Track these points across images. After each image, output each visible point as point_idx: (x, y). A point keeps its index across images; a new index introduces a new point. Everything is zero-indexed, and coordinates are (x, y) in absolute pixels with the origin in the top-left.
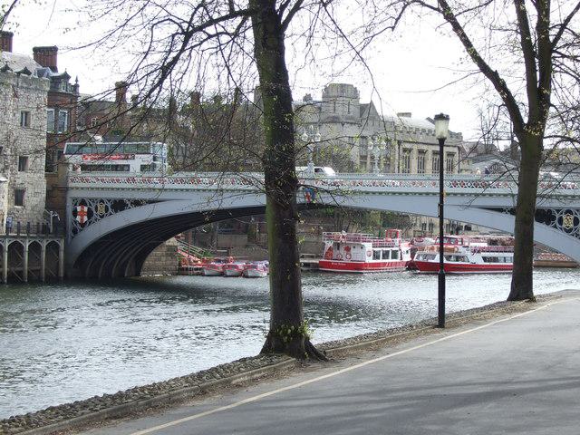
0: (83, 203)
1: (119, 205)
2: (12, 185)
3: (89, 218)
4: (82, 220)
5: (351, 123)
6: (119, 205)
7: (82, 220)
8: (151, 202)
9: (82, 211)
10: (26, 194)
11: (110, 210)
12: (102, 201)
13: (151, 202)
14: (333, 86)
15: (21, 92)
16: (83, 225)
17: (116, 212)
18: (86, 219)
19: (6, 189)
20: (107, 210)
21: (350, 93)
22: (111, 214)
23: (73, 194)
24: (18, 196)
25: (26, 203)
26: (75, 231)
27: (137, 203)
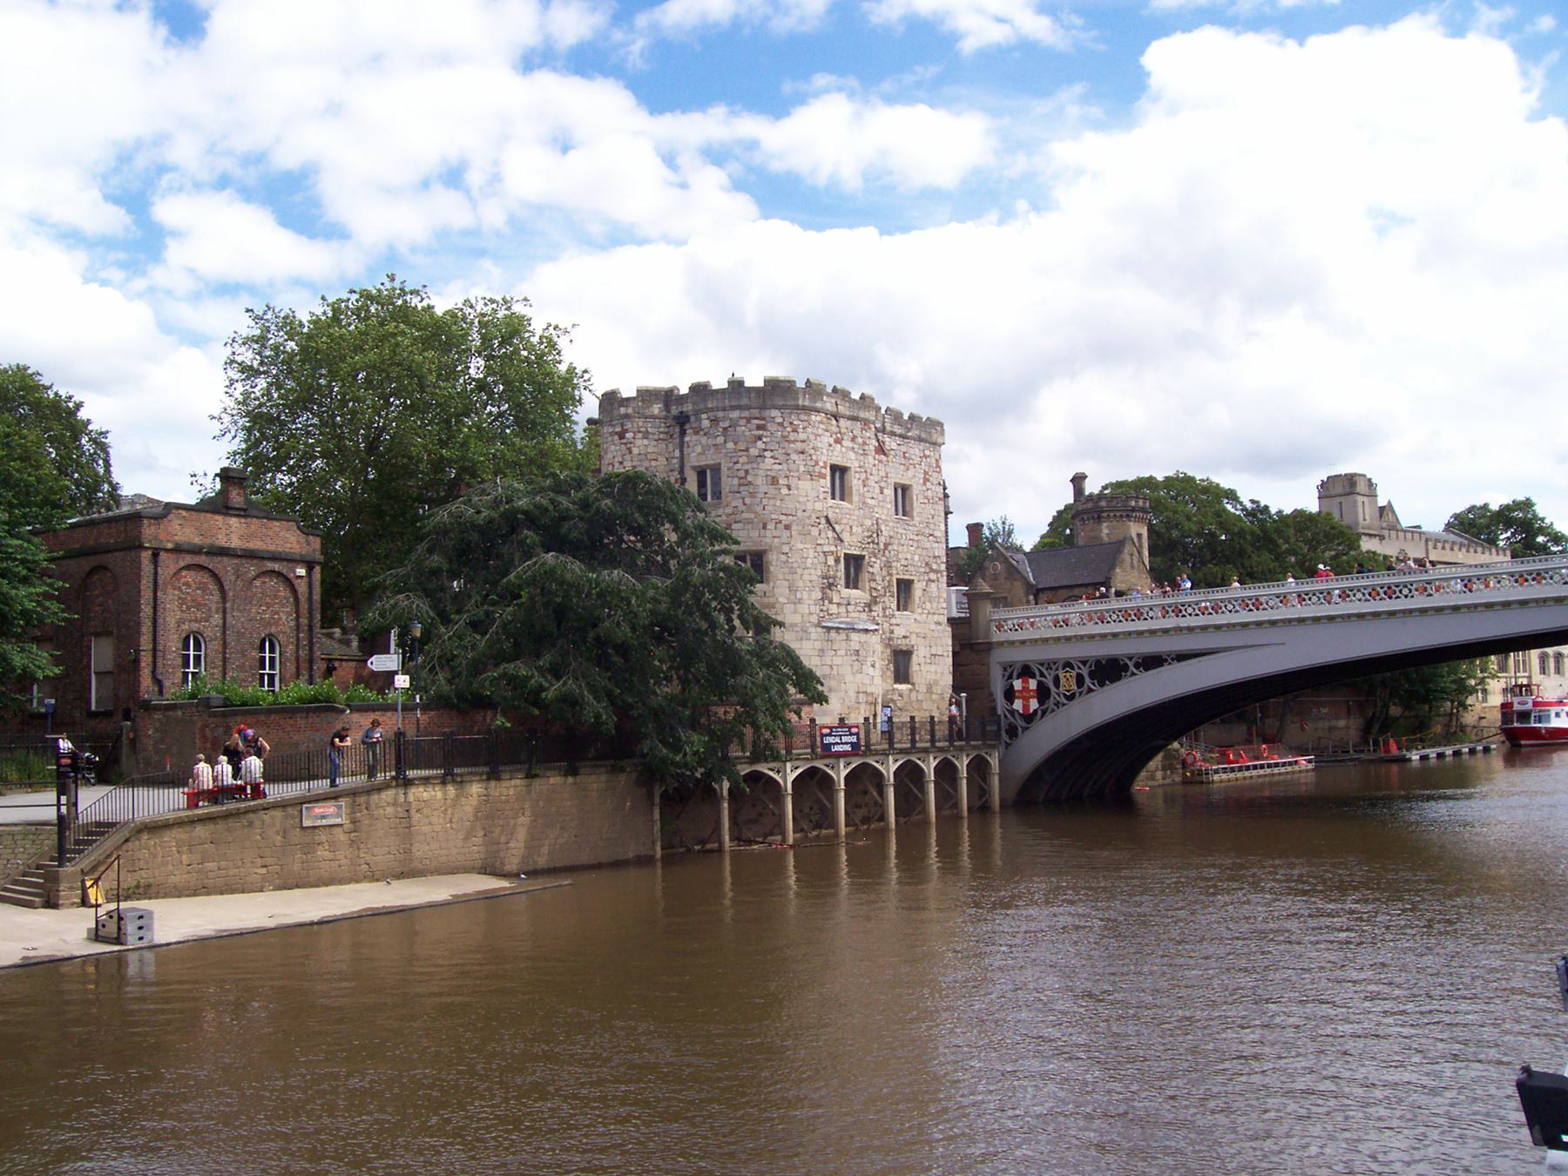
0: (1026, 672)
1: (1109, 671)
2: (888, 642)
3: (1041, 702)
4: (1026, 707)
5: (1370, 535)
6: (1109, 671)
7: (1026, 707)
8: (1182, 657)
9: (1025, 689)
10: (914, 658)
11: (1088, 681)
12: (1068, 665)
13: (1182, 657)
14: (1332, 479)
15: (890, 443)
16: (1029, 718)
17: (1102, 684)
18: (1034, 704)
19: (879, 648)
20: (1080, 680)
21: (1361, 487)
22: (1090, 690)
23: (999, 657)
24: (901, 663)
25: (916, 678)
26: (1013, 732)
27: (1151, 662)
